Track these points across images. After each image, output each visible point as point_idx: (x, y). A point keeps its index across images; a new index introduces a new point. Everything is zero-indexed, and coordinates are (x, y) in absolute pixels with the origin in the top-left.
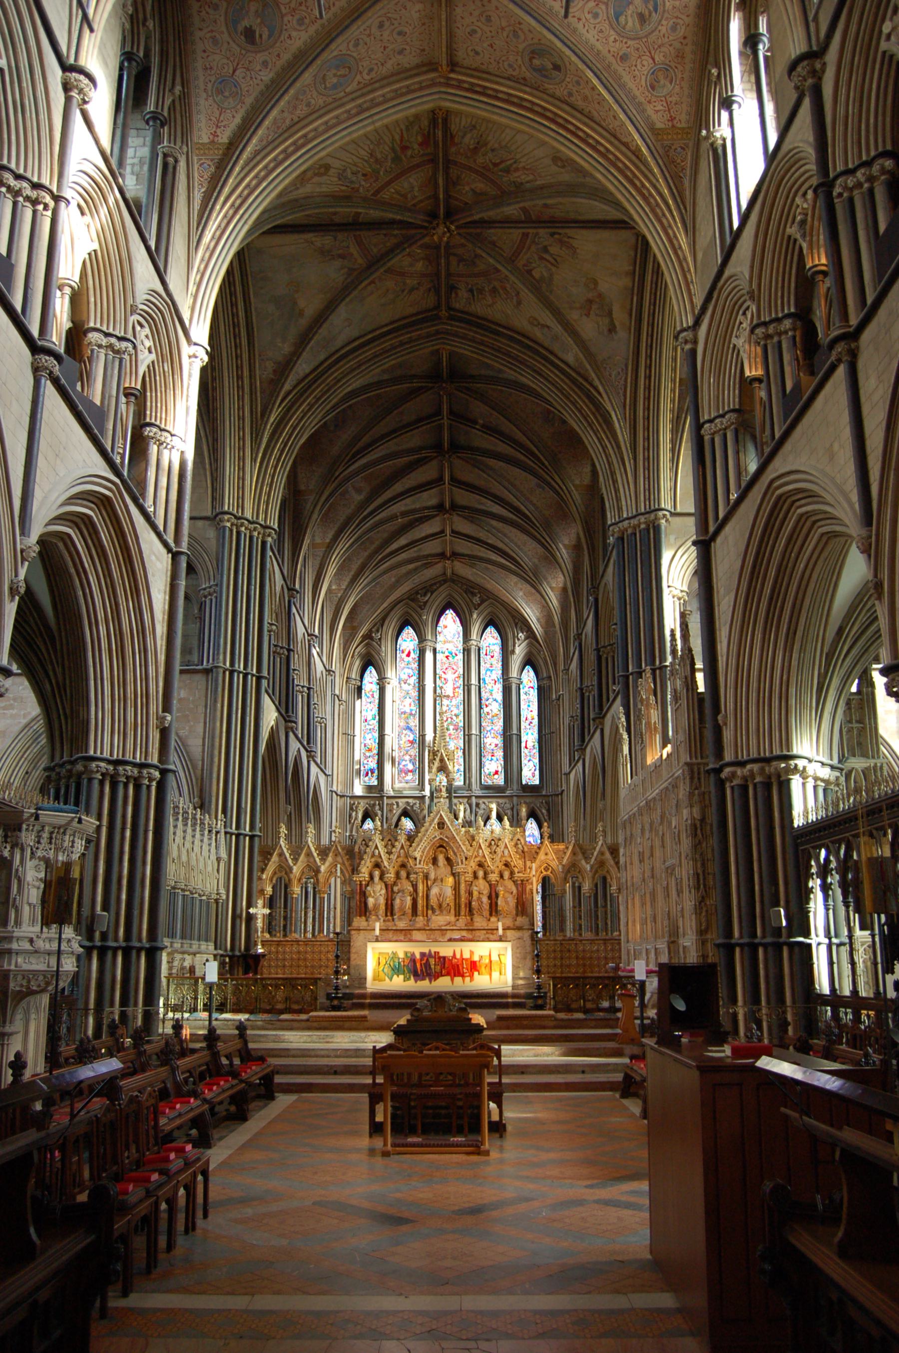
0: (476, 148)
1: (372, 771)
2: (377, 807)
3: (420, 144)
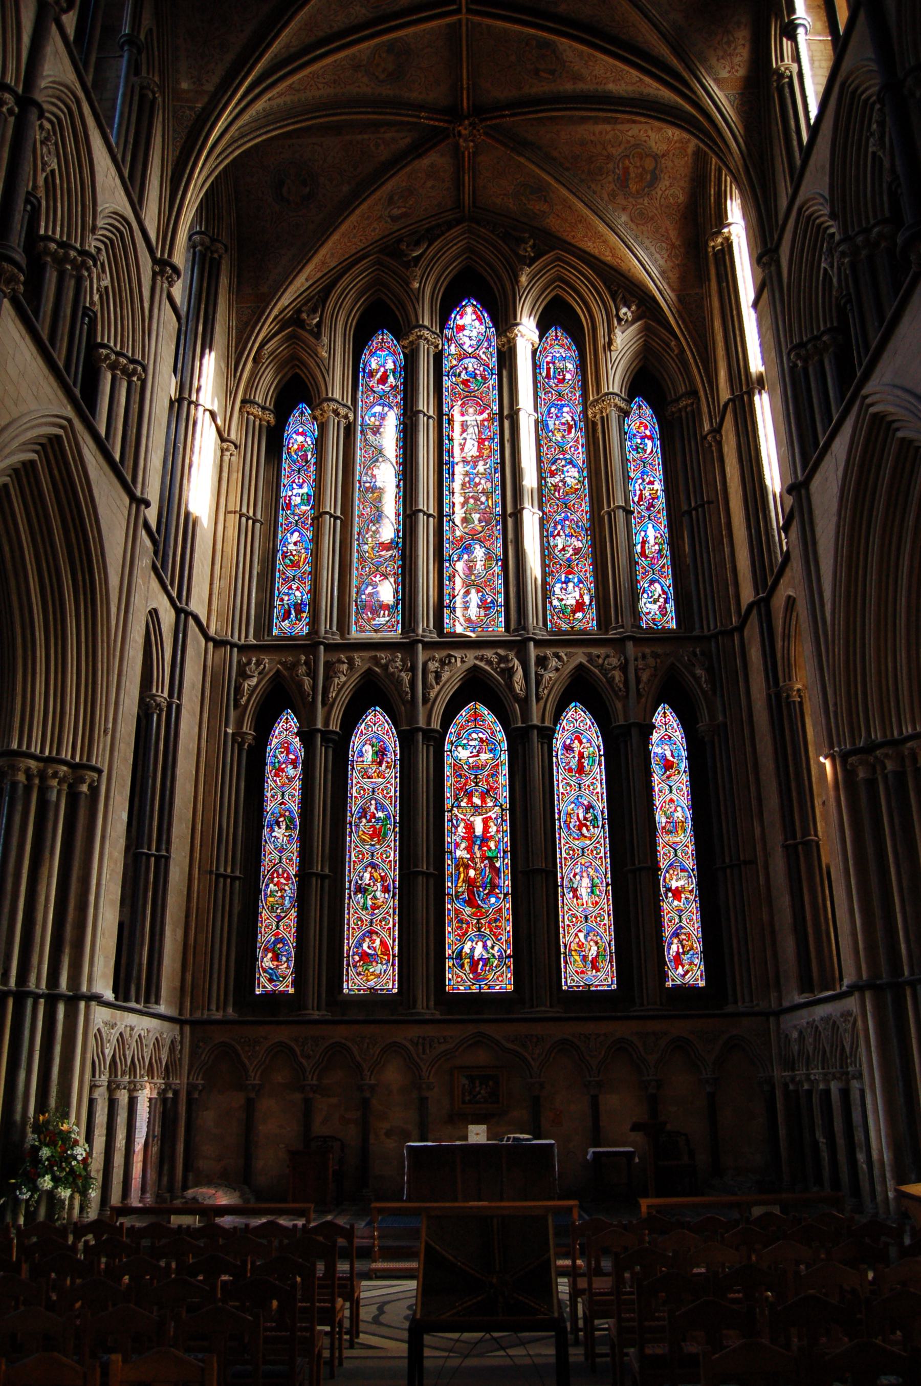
1: (299, 608)
2: (302, 670)
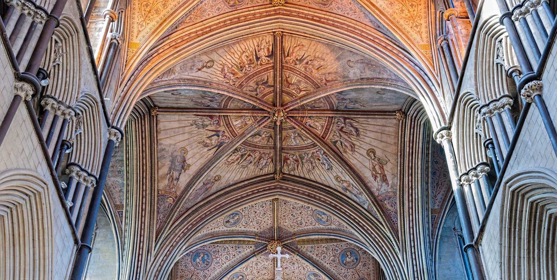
0: (260, 160)
3: (288, 159)
